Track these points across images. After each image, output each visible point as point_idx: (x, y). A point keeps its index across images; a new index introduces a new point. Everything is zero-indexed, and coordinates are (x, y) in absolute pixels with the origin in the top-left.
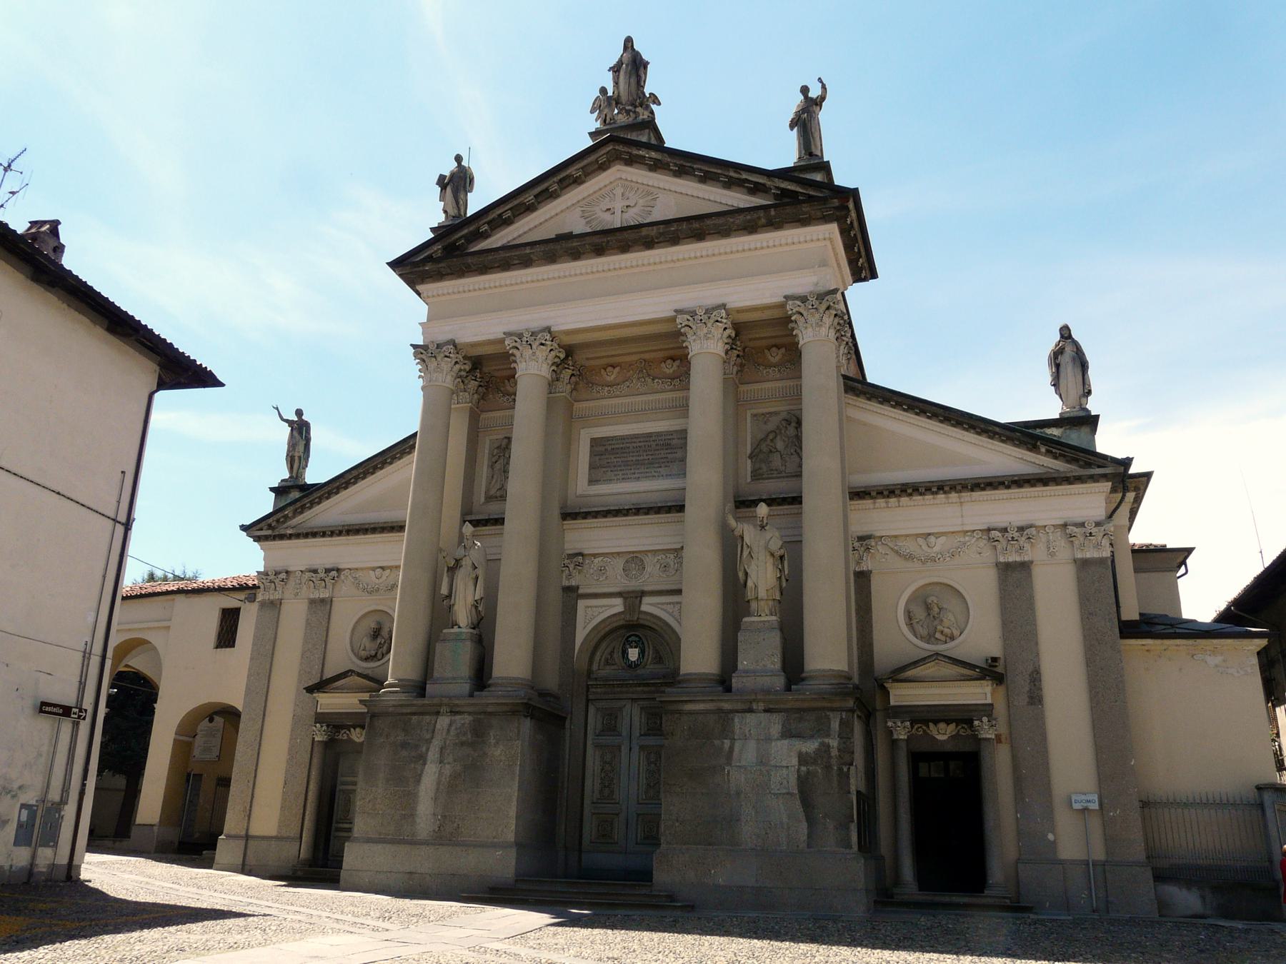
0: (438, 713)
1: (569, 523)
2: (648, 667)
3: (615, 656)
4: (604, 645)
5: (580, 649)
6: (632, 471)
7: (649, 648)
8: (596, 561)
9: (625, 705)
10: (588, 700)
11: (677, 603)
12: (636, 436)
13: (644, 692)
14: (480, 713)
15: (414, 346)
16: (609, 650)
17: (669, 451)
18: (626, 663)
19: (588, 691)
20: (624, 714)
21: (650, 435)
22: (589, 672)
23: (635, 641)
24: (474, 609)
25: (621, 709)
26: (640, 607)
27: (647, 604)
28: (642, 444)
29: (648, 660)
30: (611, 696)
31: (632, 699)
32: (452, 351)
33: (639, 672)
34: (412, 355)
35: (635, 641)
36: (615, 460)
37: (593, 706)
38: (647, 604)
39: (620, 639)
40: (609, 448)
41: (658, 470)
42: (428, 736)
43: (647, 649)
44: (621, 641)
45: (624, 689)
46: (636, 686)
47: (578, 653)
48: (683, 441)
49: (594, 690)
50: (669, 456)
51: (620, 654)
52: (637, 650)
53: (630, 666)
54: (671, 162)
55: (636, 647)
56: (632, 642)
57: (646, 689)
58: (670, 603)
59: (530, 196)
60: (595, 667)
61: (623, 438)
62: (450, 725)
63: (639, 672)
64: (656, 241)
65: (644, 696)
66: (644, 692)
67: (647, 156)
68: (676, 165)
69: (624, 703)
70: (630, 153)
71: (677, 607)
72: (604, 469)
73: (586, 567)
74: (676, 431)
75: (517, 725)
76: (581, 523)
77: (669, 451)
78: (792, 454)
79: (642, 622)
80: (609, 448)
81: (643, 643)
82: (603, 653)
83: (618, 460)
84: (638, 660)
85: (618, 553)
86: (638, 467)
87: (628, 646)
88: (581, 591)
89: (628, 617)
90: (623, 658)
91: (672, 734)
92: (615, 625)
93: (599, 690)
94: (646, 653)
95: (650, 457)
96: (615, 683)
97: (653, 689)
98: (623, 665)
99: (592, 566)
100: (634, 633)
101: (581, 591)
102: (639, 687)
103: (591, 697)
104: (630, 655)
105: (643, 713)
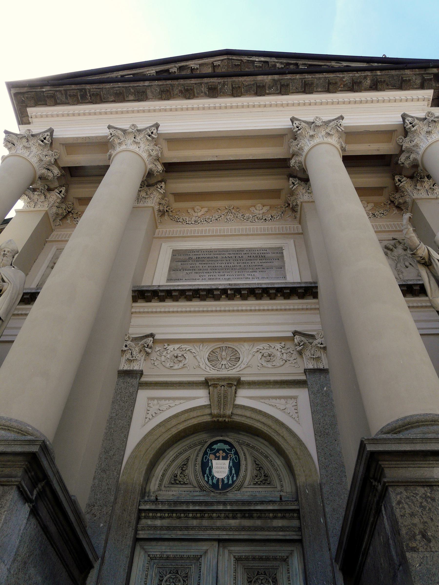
1: (141, 305)
2: (243, 490)
3: (190, 471)
4: (171, 454)
6: (221, 274)
7: (246, 459)
8: (171, 347)
9: (206, 552)
10: (137, 540)
11: (291, 398)
12: (226, 250)
13: (243, 529)
15: (6, 132)
16: (179, 461)
17: (264, 261)
18: (208, 482)
19: (139, 519)
20: (204, 569)
21: (241, 250)
22: (144, 493)
23: (224, 451)
25: (197, 558)
26: (234, 400)
27: (244, 397)
28: (232, 255)
29: (245, 477)
30: (178, 534)
31: (219, 541)
32: (47, 137)
33: (232, 496)
34: (3, 141)
35: (224, 451)
36: (201, 266)
37: (142, 553)
38: (244, 397)
39: (199, 447)
40: (194, 257)
41: (253, 274)
43: (243, 462)
44: (200, 450)
45: (205, 523)
46: (227, 517)
47: (130, 457)
48: (279, 255)
49: (149, 522)
50: (265, 265)
51: (198, 467)
52: (227, 462)
53: (215, 486)
54: (278, 62)
55: (225, 458)
56: (218, 450)
57: (247, 523)
58: (280, 398)
59: (152, 70)
60: (153, 486)
61: (210, 251)
63: (232, 496)
64: (267, 92)
65: (244, 535)
66: (243, 529)
67: (257, 60)
68: (281, 63)
69: (205, 548)
70: (241, 60)
71: (291, 402)
72: (187, 271)
73: (154, 356)
74: (270, 248)
76: (156, 307)
77: (264, 261)
78: (407, 267)
79: (237, 419)
80: (194, 257)
81: (236, 453)
82: (169, 466)
83: (205, 265)
84: (228, 477)
85: (202, 341)
86: (228, 271)
87: (212, 456)
88: (143, 379)
89: (215, 411)
90: (204, 473)
91: (424, 536)
92: (195, 422)
93: (158, 523)
94: (243, 468)
95: (243, 265)
96: (191, 508)
97: (258, 523)
98: (203, 483)
99: (164, 353)
100: (221, 438)
101: (143, 379)
102: (234, 518)
103: (142, 534)
104: (214, 470)
105: (240, 570)
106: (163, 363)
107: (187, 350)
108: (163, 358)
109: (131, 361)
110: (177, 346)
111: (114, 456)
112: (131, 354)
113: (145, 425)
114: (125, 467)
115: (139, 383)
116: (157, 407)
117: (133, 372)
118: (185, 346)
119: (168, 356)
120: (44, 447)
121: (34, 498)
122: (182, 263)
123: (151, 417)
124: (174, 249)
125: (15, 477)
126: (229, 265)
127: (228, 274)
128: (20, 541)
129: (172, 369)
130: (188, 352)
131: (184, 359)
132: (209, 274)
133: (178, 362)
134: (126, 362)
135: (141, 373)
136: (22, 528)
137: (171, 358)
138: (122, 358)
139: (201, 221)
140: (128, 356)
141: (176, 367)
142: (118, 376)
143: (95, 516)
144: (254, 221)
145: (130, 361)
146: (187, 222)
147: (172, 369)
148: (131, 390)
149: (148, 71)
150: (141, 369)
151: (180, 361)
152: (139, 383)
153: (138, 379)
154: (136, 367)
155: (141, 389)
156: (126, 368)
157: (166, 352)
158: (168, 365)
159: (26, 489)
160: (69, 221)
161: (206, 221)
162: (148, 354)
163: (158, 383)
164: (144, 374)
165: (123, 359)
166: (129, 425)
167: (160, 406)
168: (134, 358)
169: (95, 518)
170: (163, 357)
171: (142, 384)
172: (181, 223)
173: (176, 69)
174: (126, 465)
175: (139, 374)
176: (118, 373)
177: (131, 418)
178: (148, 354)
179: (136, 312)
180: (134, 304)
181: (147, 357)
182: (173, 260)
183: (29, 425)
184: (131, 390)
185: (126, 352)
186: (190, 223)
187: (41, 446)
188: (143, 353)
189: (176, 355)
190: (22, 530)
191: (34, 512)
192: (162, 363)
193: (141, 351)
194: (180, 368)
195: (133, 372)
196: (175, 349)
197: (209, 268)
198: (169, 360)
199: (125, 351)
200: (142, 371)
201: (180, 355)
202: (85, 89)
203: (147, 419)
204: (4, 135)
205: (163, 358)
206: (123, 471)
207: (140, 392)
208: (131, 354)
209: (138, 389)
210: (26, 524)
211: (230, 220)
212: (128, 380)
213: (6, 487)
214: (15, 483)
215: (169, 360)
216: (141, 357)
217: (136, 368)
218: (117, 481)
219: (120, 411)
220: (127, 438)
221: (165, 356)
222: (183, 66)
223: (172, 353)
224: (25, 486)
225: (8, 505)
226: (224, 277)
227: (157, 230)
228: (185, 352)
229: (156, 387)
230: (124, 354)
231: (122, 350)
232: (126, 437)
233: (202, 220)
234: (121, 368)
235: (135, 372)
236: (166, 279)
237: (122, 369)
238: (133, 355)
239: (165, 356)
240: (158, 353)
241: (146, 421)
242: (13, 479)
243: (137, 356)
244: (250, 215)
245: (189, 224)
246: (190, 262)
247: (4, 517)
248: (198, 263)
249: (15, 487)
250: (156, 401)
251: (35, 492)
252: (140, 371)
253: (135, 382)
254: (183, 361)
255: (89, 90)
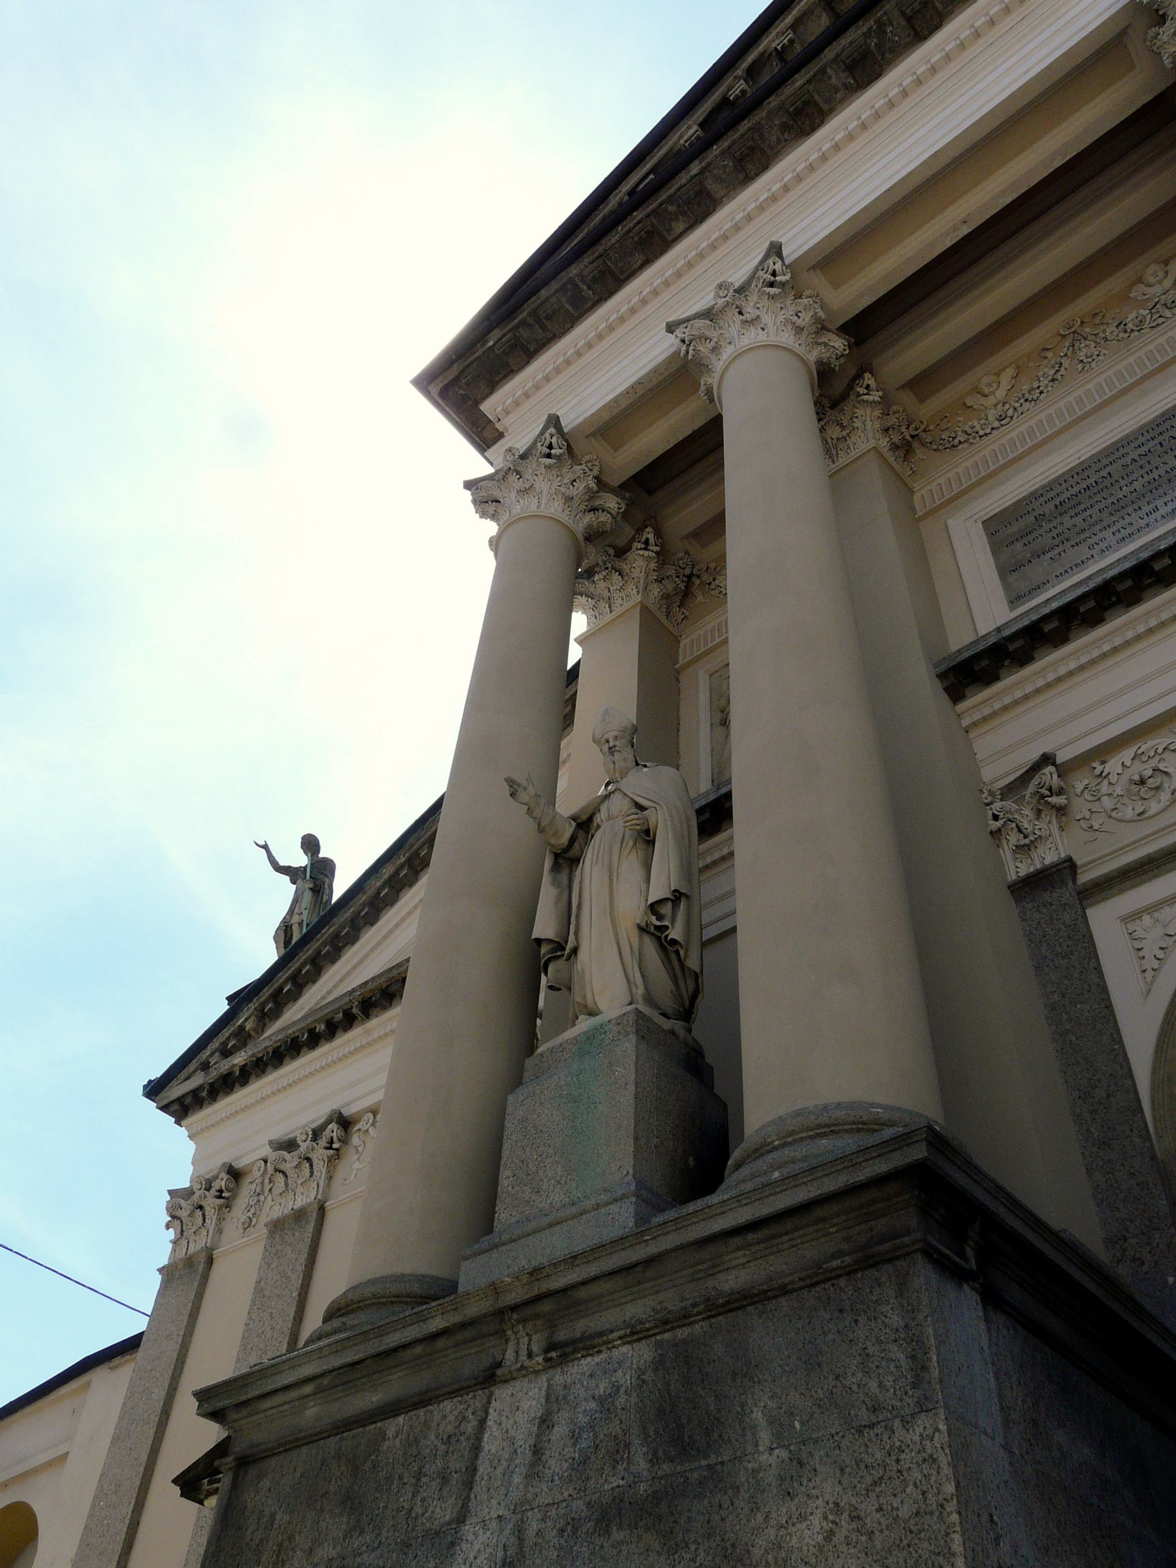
0: (490, 1378)
1: (979, 701)
5: (1154, 1072)
6: (1146, 509)
8: (1113, 765)
14: (684, 1318)
15: (469, 485)
24: (651, 949)
32: (554, 440)
34: (471, 508)
36: (1078, 520)
42: (443, 1512)
47: (1154, 1087)
59: (689, 128)
61: (1082, 469)
62: (545, 1422)
72: (1049, 555)
73: (1080, 807)
75: (896, 1320)
76: (1018, 683)
83: (1088, 513)
86: (1161, 491)
88: (1084, 878)
101: (1084, 878)
106: (1114, 814)
107: (1160, 751)
108: (1107, 803)
109: (1027, 848)
110: (1127, 755)
111: (1112, 1099)
112: (1020, 831)
113: (1149, 991)
114: (1154, 1116)
115: (1079, 893)
116: (1159, 931)
117: (1049, 872)
118: (1150, 743)
119: (1119, 790)
120: (936, 1140)
121: (974, 1267)
122: (1025, 540)
123: (1156, 964)
124: (986, 518)
125: (908, 1232)
126: (1155, 474)
127: (1166, 499)
128: (996, 1375)
129: (1148, 818)
130: (1166, 755)
131: (1165, 778)
132: (1114, 529)
133: (1153, 793)
134: (1018, 856)
135: (1069, 866)
136: (985, 1343)
137: (1128, 790)
138: (1001, 851)
139: (1015, 409)
140: (1014, 838)
141: (1154, 807)
142: (1015, 898)
143: (1143, 1263)
144: (1161, 320)
145: (1023, 849)
146: (981, 433)
147: (1148, 818)
148: (1067, 918)
149: (681, 137)
150: (1063, 856)
151: (1157, 788)
152: (1079, 893)
153: (1070, 884)
154: (1047, 856)
155: (1093, 904)
156: (1025, 869)
157: (1106, 782)
158: (1129, 813)
159: (948, 1252)
160: (700, 598)
161: (1026, 400)
162: (1061, 810)
163: (1129, 871)
164: (1078, 863)
165: (1006, 853)
166: (1109, 1007)
167: (1165, 926)
168: (1032, 838)
169: (1145, 1268)
170: (1105, 799)
171: (1087, 890)
172: (965, 445)
173: (742, 81)
174: (1153, 1109)
175: (1067, 871)
176: (1012, 892)
177: (1104, 989)
178: (1061, 810)
179: (975, 724)
180: (962, 706)
181: (1064, 818)
182: (996, 548)
183: (872, 1105)
184: (1067, 918)
185: (1004, 833)
186: (988, 431)
187: (929, 1143)
188: (1049, 816)
189: (1136, 778)
190: (986, 1347)
191: (992, 1300)
192: (1110, 817)
193: (1039, 811)
194: (1168, 806)
195: (1049, 872)
196: (1128, 763)
197: (1105, 514)
198: (1125, 800)
199: (999, 830)
200: (1070, 860)
201: (1149, 773)
202: (571, 281)
203: (1149, 975)
204: (468, 495)
205: (1107, 803)
206: (1156, 1128)
207: (1089, 912)
208: (1020, 831)
209: (1084, 909)
210: (989, 1330)
211: (1090, 360)
212: (1046, 896)
213: (898, 1263)
214: (913, 1248)
215: (1125, 800)
216: (1047, 825)
217: (1050, 858)
218: (1153, 1158)
219: (1066, 981)
220: (1121, 1042)
221: (1109, 795)
222: (754, 62)
223: (1125, 779)
224: (940, 1247)
225: (925, 1301)
226: (1157, 515)
227: (916, 498)
228: (1157, 758)
229: (1128, 883)
230: (999, 839)
231: (991, 833)
232: (1116, 1037)
233: (1017, 405)
234: (1012, 876)
235: (1054, 870)
236: (1005, 602)
237: (1014, 877)
238: (1025, 831)
239: (1109, 795)
240: (1087, 795)
241: (1149, 979)
242: (906, 1240)
243: (1037, 827)
244: (1142, 312)
245: (986, 435)
246: (1046, 527)
247: (930, 1330)
248: (1066, 519)
249: (919, 1255)
250: (1147, 919)
251: (969, 1252)
252: (1066, 861)
253: (1066, 894)
254: (1166, 785)
255: (580, 275)
